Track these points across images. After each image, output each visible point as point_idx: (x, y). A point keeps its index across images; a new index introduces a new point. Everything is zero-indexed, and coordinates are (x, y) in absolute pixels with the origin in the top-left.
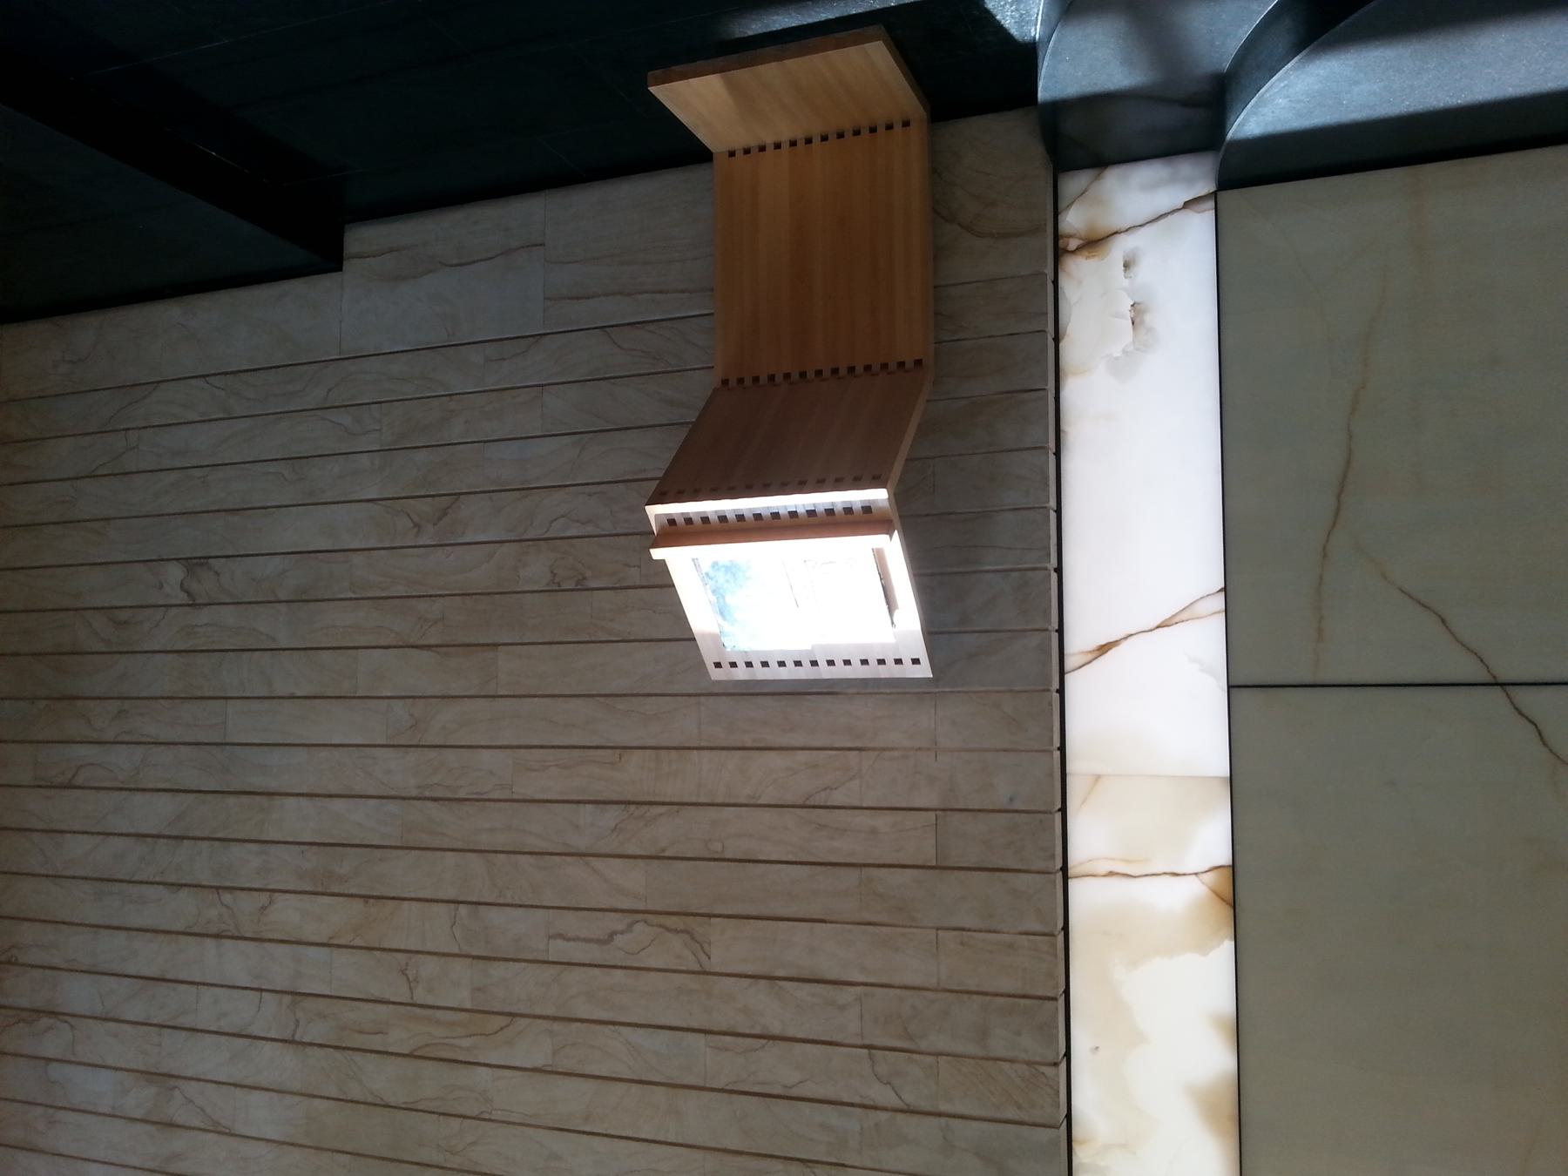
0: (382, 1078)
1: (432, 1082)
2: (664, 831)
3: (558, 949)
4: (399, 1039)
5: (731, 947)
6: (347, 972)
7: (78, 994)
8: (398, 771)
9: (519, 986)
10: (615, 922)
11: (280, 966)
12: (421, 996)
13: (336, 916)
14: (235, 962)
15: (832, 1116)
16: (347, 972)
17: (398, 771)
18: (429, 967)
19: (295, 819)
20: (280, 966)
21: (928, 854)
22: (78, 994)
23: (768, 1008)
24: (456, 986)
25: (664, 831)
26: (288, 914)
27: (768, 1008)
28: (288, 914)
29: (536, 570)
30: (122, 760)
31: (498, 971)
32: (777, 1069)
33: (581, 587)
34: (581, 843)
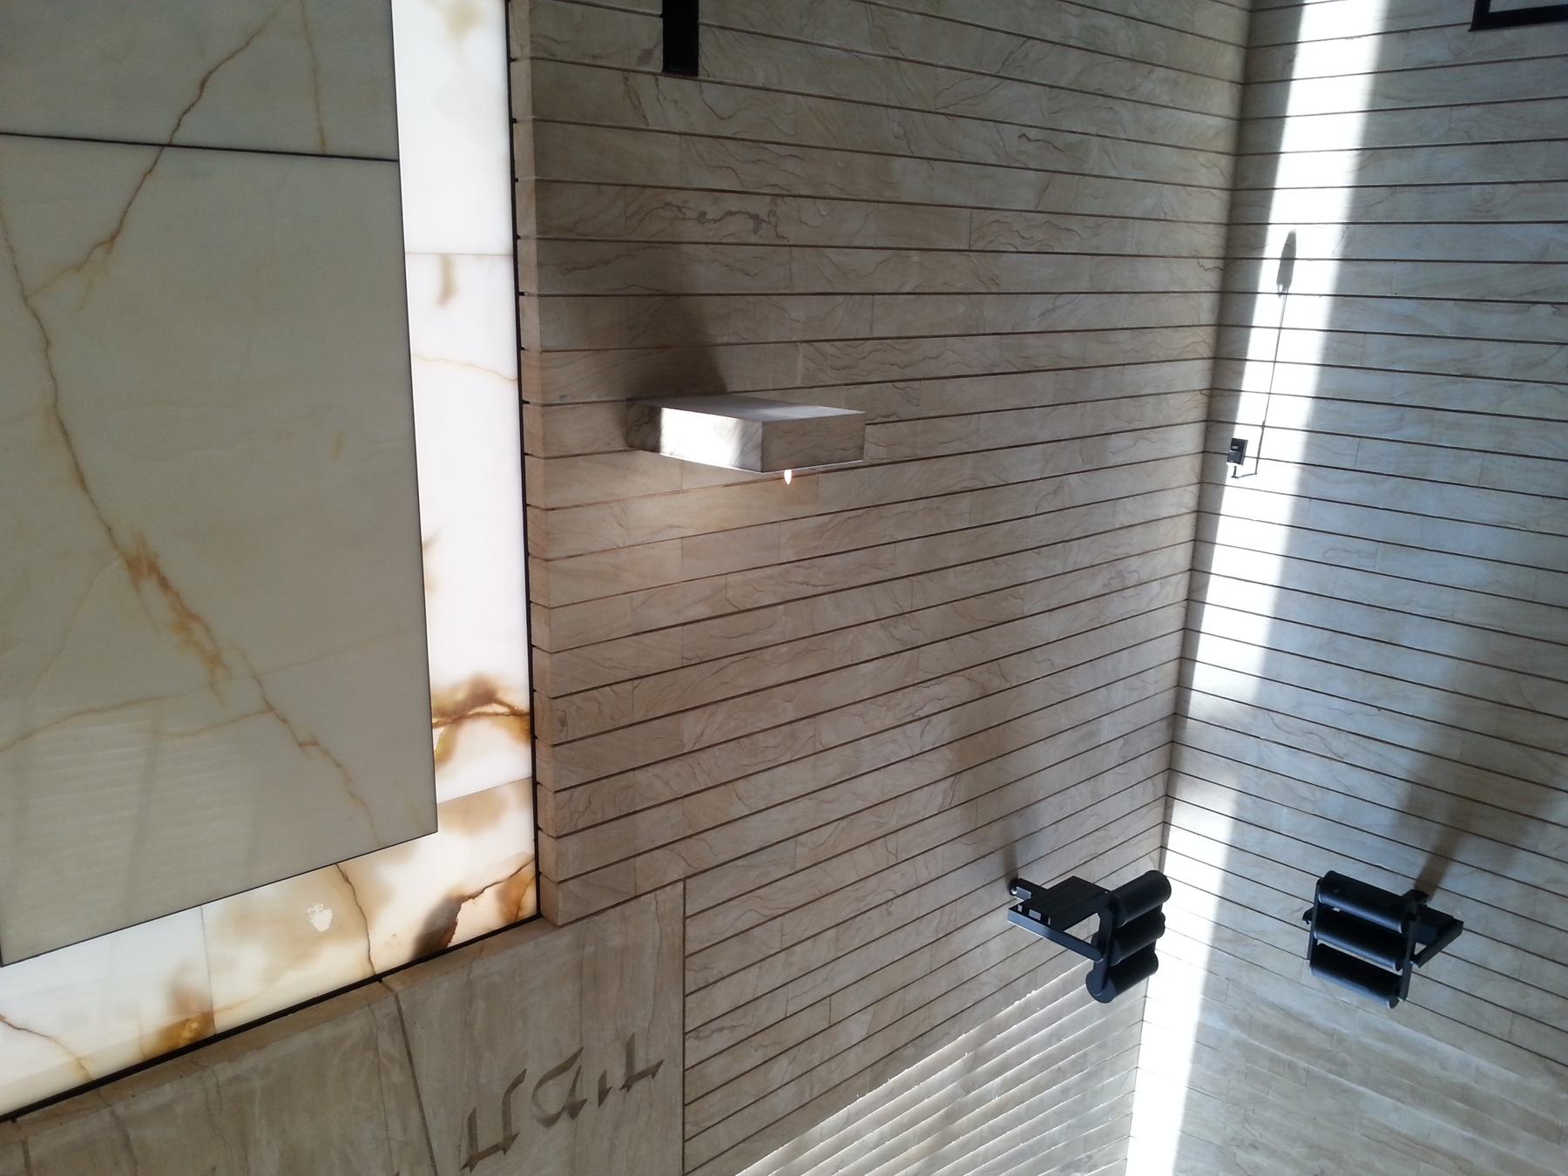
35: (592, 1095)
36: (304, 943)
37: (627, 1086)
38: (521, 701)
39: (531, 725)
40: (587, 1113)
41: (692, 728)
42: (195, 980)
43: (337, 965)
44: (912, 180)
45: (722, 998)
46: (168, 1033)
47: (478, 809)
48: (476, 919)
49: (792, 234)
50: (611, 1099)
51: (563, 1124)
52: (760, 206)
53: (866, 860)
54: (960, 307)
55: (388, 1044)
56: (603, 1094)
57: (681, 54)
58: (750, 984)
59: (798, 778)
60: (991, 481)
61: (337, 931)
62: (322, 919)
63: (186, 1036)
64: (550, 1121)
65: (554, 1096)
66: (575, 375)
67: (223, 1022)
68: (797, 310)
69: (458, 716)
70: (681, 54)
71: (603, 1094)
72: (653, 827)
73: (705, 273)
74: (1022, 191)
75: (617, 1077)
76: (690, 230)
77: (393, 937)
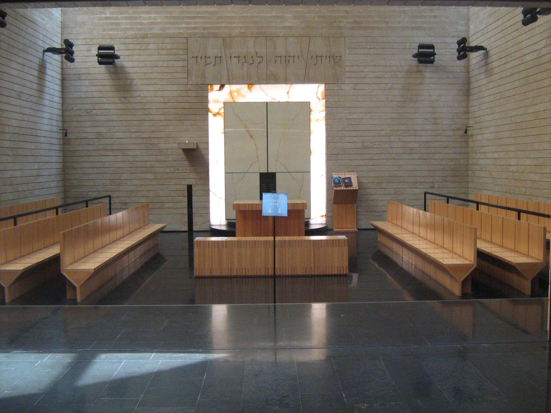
0: (403, 127)
1: (396, 128)
2: (367, 157)
3: (380, 143)
4: (400, 132)
5: (360, 145)
6: (408, 139)
7: (450, 133)
8: (402, 162)
9: (384, 139)
10: (374, 147)
11: (417, 139)
12: (398, 137)
13: (410, 145)
14: (424, 139)
15: (348, 129)
16: (408, 139)
17: (402, 162)
18: (396, 141)
19: (416, 156)
20: (417, 139)
21: (339, 156)
22: (450, 133)
23: (355, 139)
24: (393, 138)
25: (367, 157)
26: (416, 145)
27: (355, 139)
28: (416, 145)
29: (383, 185)
30: (444, 162)
31: (387, 141)
32: (355, 133)
33: (378, 183)
34: (377, 155)
35: (203, 58)
36: (238, 91)
37: (197, 57)
38: (209, 113)
39: (207, 110)
40: (203, 56)
41: (187, 106)
42: (249, 91)
43: (234, 87)
44: (150, 176)
45: (181, 64)
46: (252, 87)
47: (216, 101)
48: (217, 87)
49: (172, 168)
50: (200, 56)
51: (208, 56)
52: (177, 171)
53: (152, 76)
54: (138, 159)
55: (230, 78)
56: (201, 57)
57: (190, 188)
58: (176, 64)
59: (167, 94)
60: (127, 133)
61: (234, 91)
62: (235, 94)
63: (250, 86)
64: (209, 57)
65: (208, 61)
66: (204, 152)
67: (247, 86)
68: (170, 159)
69: (218, 114)
70: (190, 188)
71: (201, 57)
72: (194, 94)
73: (186, 163)
74: (124, 176)
75: (199, 59)
76: (188, 168)
77: (227, 88)
